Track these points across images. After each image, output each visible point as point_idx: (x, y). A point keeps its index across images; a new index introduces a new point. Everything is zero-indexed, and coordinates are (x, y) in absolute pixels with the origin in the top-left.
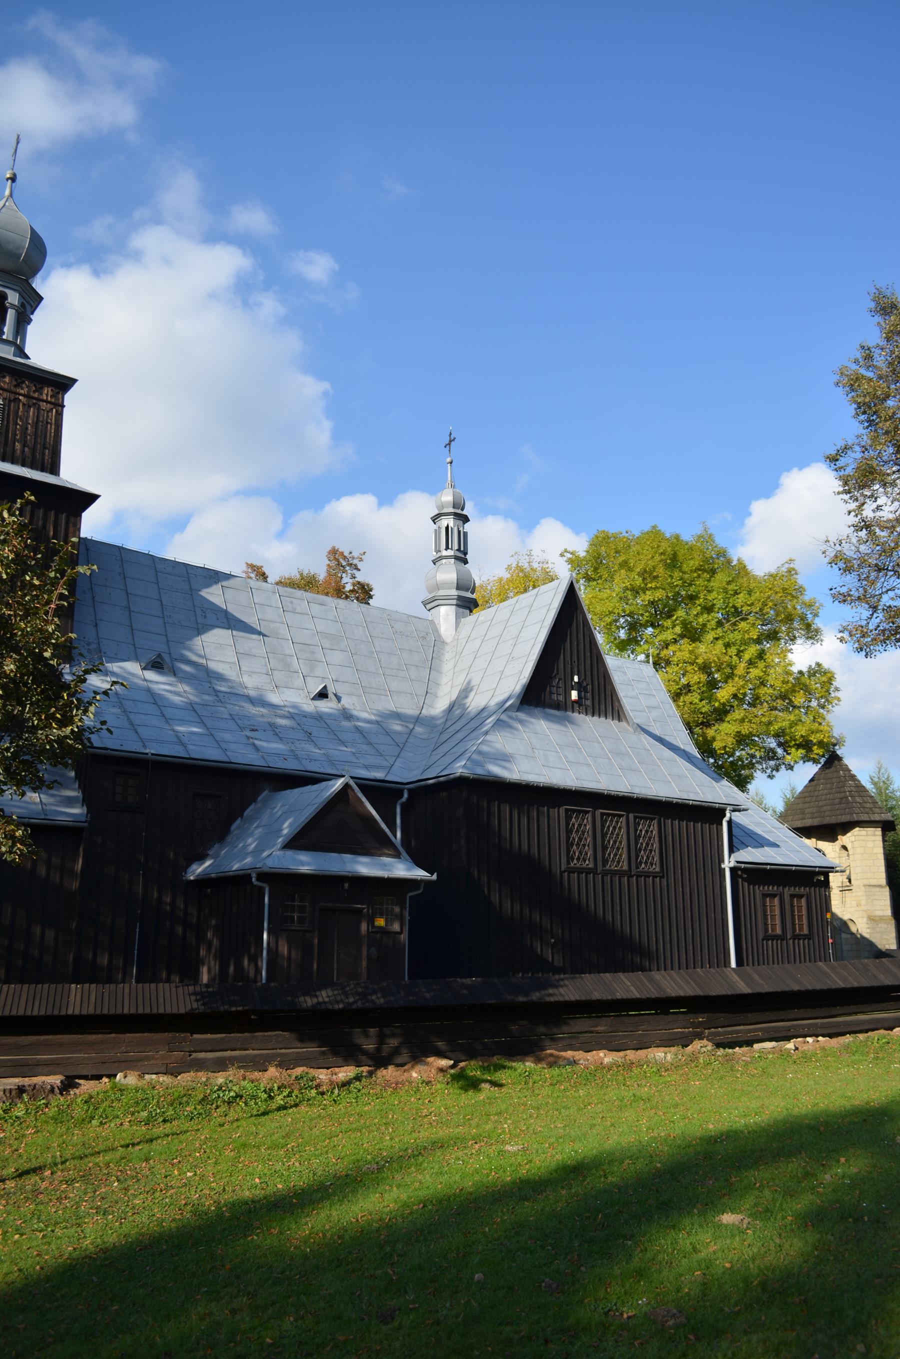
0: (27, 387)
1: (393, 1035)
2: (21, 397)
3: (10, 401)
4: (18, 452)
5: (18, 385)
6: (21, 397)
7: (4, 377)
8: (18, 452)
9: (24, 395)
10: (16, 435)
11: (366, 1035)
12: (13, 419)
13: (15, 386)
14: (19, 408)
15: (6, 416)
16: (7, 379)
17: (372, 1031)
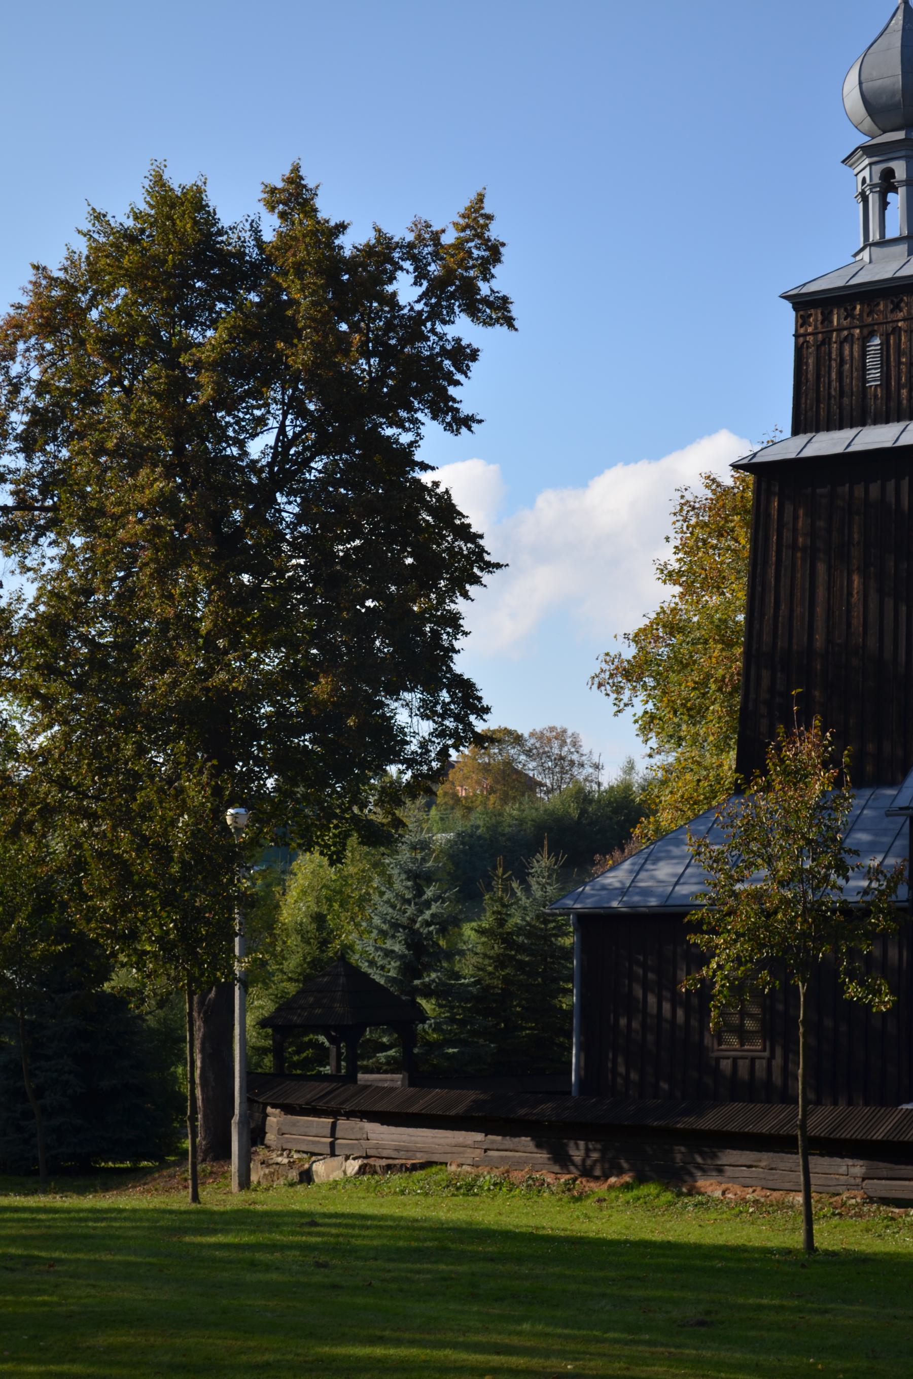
0: (907, 305)
1: (595, 1150)
2: (900, 324)
3: (888, 336)
4: (905, 402)
5: (897, 307)
6: (900, 324)
7: (878, 304)
8: (905, 402)
9: (904, 320)
10: (899, 379)
11: (578, 1148)
12: (894, 359)
13: (892, 311)
14: (900, 340)
15: (885, 358)
16: (881, 307)
17: (582, 1144)
